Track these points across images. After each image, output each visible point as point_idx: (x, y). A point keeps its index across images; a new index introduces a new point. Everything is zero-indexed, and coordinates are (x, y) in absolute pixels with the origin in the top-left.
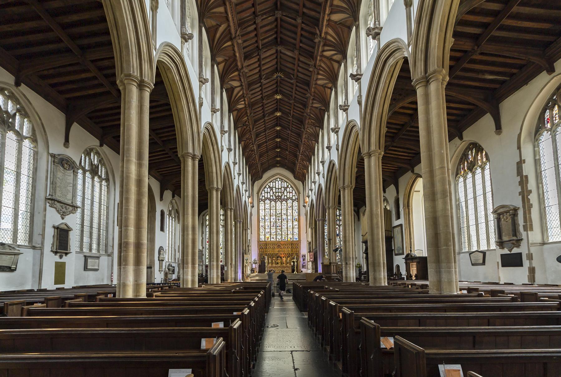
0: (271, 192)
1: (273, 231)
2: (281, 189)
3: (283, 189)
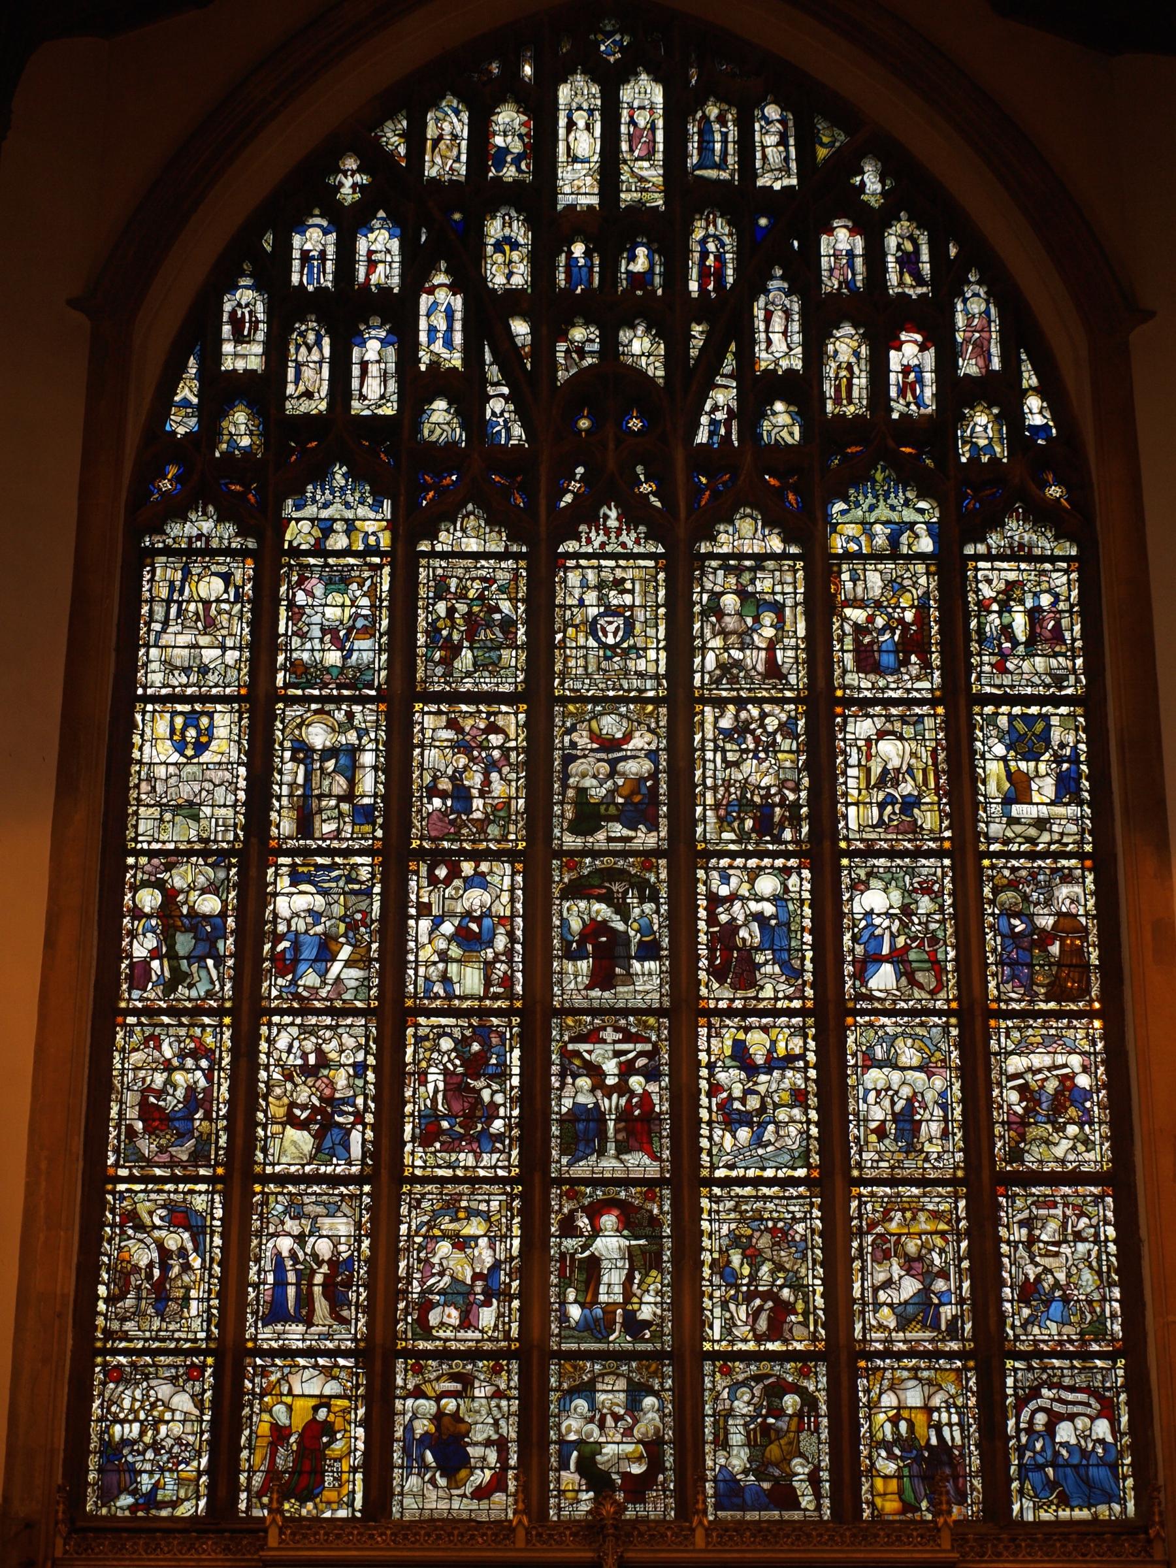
0: (440, 308)
1: (467, 1248)
2: (667, 231)
3: (713, 237)
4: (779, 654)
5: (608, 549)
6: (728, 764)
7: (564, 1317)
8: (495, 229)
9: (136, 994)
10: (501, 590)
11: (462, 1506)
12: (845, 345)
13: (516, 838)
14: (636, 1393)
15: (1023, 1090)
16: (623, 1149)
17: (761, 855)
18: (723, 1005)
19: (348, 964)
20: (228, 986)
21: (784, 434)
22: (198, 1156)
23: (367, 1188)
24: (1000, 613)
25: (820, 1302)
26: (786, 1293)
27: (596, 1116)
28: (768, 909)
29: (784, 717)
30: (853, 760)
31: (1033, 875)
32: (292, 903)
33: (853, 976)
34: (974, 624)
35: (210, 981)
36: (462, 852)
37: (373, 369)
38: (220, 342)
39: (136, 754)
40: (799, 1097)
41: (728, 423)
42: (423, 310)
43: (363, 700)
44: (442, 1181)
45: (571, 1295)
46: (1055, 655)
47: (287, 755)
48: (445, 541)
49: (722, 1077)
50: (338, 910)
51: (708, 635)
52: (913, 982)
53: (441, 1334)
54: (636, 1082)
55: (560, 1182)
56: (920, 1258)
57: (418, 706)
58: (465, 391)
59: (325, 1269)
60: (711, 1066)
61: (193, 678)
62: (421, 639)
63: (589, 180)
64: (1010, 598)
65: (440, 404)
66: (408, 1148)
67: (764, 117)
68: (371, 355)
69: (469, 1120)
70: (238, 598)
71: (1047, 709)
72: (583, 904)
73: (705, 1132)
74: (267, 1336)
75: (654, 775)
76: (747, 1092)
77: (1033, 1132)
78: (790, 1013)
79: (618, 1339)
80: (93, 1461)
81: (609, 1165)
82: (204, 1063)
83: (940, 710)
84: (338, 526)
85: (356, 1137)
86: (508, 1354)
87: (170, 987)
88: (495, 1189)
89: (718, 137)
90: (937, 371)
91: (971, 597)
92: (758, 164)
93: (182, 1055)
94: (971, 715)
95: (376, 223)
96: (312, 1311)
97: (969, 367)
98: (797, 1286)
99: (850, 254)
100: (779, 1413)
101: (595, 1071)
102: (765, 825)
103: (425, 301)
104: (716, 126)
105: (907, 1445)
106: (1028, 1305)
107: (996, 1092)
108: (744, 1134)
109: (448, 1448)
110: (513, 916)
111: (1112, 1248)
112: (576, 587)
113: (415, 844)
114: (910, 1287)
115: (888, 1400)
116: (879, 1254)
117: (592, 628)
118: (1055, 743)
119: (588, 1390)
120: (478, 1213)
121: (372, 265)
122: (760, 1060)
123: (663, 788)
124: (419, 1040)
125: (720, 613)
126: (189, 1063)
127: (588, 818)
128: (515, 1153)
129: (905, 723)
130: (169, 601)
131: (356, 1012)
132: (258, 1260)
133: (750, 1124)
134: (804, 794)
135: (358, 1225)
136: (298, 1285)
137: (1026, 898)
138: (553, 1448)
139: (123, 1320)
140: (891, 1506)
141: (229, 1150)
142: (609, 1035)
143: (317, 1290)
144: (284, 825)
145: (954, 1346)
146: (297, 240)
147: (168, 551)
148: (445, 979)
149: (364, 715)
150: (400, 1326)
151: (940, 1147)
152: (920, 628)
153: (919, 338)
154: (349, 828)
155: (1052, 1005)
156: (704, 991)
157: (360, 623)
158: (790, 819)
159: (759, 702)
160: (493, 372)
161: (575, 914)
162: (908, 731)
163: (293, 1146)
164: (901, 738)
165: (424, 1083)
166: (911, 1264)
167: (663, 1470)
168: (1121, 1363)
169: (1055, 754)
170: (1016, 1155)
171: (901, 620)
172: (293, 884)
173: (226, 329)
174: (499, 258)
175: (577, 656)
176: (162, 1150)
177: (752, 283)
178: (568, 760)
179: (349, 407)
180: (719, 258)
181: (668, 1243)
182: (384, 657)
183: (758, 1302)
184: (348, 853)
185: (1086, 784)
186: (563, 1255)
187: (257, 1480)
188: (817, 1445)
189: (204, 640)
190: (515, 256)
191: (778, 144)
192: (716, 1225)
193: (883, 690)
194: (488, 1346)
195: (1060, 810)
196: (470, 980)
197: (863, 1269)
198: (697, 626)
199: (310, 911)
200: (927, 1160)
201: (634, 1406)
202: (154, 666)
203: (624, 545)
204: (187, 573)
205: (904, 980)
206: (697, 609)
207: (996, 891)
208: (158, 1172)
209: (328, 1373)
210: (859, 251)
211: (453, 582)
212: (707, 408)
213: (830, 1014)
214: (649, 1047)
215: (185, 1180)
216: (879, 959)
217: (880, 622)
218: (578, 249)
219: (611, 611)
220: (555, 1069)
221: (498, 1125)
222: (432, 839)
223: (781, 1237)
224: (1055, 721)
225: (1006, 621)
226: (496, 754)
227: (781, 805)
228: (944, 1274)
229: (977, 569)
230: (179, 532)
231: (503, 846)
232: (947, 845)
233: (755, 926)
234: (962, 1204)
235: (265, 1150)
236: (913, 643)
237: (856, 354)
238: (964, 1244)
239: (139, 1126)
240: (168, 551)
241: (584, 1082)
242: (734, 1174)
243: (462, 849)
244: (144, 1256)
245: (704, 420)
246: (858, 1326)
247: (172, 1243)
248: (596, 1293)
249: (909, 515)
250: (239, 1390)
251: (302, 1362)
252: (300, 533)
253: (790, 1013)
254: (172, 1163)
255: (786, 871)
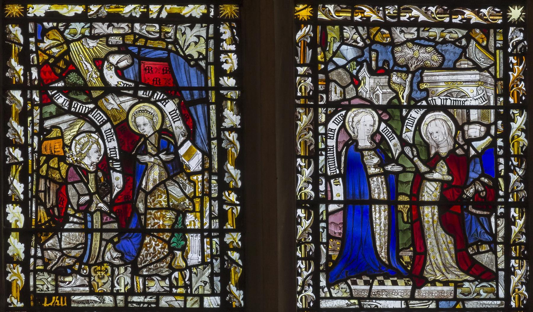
59: (441, 172)
96: (421, 255)
132: (312, 156)
136: (392, 203)
139: (60, 272)
143: (429, 214)
247: (144, 124)
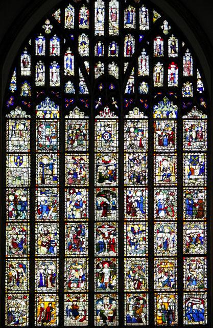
0: (69, 58)
1: (77, 271)
2: (119, 40)
3: (130, 41)
4: (142, 142)
5: (106, 117)
6: (131, 167)
7: (97, 285)
8: (81, 40)
9: (10, 218)
10: (83, 127)
11: (78, 323)
12: (159, 68)
13: (87, 183)
14: (111, 300)
15: (190, 237)
16: (109, 250)
17: (137, 187)
18: (129, 220)
19: (53, 212)
20: (29, 216)
21: (144, 90)
22: (24, 253)
23: (58, 259)
24: (190, 132)
25: (147, 282)
26: (141, 280)
27: (103, 243)
28: (139, 199)
29: (143, 156)
30: (157, 166)
31: (194, 191)
32: (41, 199)
33: (156, 213)
34: (184, 135)
35: (25, 216)
36: (76, 187)
37: (55, 74)
38: (20, 67)
39: (7, 165)
40: (144, 239)
41: (132, 87)
42: (65, 60)
43: (54, 153)
44: (73, 257)
45: (98, 280)
46: (201, 142)
47: (39, 165)
48: (71, 115)
49: (129, 235)
50: (50, 200)
51: (127, 137)
52: (168, 215)
53: (73, 289)
54: (112, 236)
55: (96, 257)
56: (167, 272)
57: (66, 154)
58: (75, 80)
59: (50, 276)
60: (127, 233)
61: (18, 148)
62: (66, 139)
63: (102, 27)
64: (192, 129)
65: (69, 83)
66: (66, 251)
67: (142, 11)
68: (54, 71)
69: (78, 245)
70: (27, 129)
71: (199, 154)
72: (101, 198)
73: (125, 246)
74: (39, 290)
75: (116, 170)
76: (134, 238)
77: (191, 246)
78: (143, 221)
79: (108, 290)
80: (6, 315)
81: (106, 254)
82: (24, 233)
83: (176, 154)
84: (48, 112)
85: (55, 249)
86: (86, 293)
87: (17, 217)
88: (83, 259)
89: (131, 16)
90: (179, 74)
91: (184, 128)
92: (140, 23)
93: (20, 232)
94: (182, 155)
95: (54, 38)
96: (48, 285)
97: (186, 74)
98: (143, 278)
99: (160, 45)
100: (139, 304)
101: (103, 234)
102: (139, 181)
103: (65, 57)
104: (131, 13)
105: (164, 310)
106: (189, 282)
107: (184, 238)
108: (133, 247)
109: (75, 312)
110: (86, 201)
111: (206, 270)
112: (99, 126)
113: (66, 185)
114: (165, 278)
115: (160, 301)
116: (159, 272)
117: (103, 136)
118: (200, 162)
119: (102, 300)
120: (80, 264)
121: (53, 48)
122: (137, 231)
123: (117, 173)
124: (68, 228)
125: (130, 132)
126: (21, 233)
127: (102, 179)
128: (87, 251)
129: (168, 157)
130: (12, 130)
131: (55, 222)
132: (37, 274)
133: (134, 245)
134: (147, 174)
135: (56, 267)
136: (45, 279)
137: (192, 196)
138: (95, 311)
139: (11, 287)
140: (160, 322)
141: (30, 251)
142: (106, 226)
143: (49, 280)
144: (39, 181)
145: (174, 290)
146: (37, 42)
147: (11, 118)
148: (73, 215)
149: (55, 156)
150: (65, 287)
151: (173, 250)
152: (173, 136)
153: (175, 66)
154: (52, 182)
155: (196, 219)
156: (125, 217)
157: (53, 135)
158: (144, 179)
159: (138, 153)
160: (81, 75)
161: (99, 200)
162: (169, 159)
163: (43, 251)
164: (168, 161)
165: (69, 237)
166: (165, 273)
167: (116, 315)
168: (206, 293)
169: (200, 164)
170: (187, 251)
171: (168, 134)
172: (41, 194)
173: (22, 65)
174: (82, 46)
175: (100, 143)
176: (17, 251)
177: (138, 53)
178: (98, 166)
179: (49, 84)
180: (131, 46)
181: (118, 270)
182: (59, 143)
183: (135, 282)
184: (52, 187)
185: (206, 171)
186: (97, 272)
187: (38, 319)
188: (146, 310)
189: (20, 139)
190: (85, 46)
191: (145, 18)
192: (127, 265)
193: (164, 150)
194: (82, 291)
195: (200, 177)
196: (78, 215)
197: (156, 275)
198: (125, 135)
199: (45, 200)
200: (169, 252)
201: (111, 303)
202: (9, 145)
203: (109, 116)
204: (16, 123)
205: (166, 214)
206: (125, 131)
207: (186, 195)
208: (16, 256)
209: (51, 297)
210: (162, 45)
211: (73, 125)
212: (128, 84)
213: (151, 222)
214: (114, 229)
215: (22, 258)
216: (161, 210)
217: (164, 134)
218: (99, 44)
219: (107, 132)
220: (95, 234)
221: (84, 246)
222: (69, 184)
223: (140, 268)
224: (200, 156)
225: (191, 134)
226: (83, 165)
227: (142, 176)
228: (172, 276)
229: (185, 122)
230: (13, 113)
231: (84, 185)
232: (176, 184)
233: (136, 203)
234: (176, 261)
235: (37, 251)
236: (171, 139)
237: (161, 70)
238: (176, 269)
239: (12, 247)
240: (11, 118)
241: (101, 236)
242: (131, 255)
243: (76, 186)
244: (14, 273)
245: (127, 86)
246: (155, 286)
247: (19, 271)
248: (103, 280)
249: (171, 109)
250: (34, 301)
251: (46, 295)
252: (40, 114)
253: (143, 221)
254: (19, 254)
255: (143, 190)
